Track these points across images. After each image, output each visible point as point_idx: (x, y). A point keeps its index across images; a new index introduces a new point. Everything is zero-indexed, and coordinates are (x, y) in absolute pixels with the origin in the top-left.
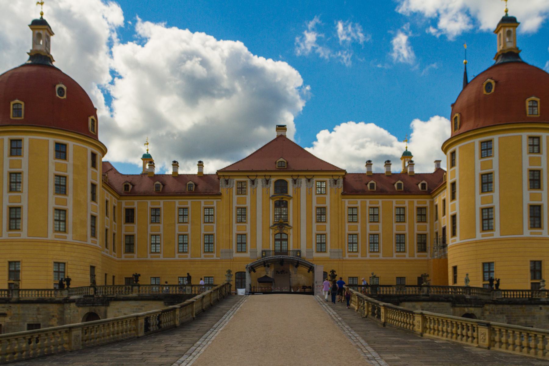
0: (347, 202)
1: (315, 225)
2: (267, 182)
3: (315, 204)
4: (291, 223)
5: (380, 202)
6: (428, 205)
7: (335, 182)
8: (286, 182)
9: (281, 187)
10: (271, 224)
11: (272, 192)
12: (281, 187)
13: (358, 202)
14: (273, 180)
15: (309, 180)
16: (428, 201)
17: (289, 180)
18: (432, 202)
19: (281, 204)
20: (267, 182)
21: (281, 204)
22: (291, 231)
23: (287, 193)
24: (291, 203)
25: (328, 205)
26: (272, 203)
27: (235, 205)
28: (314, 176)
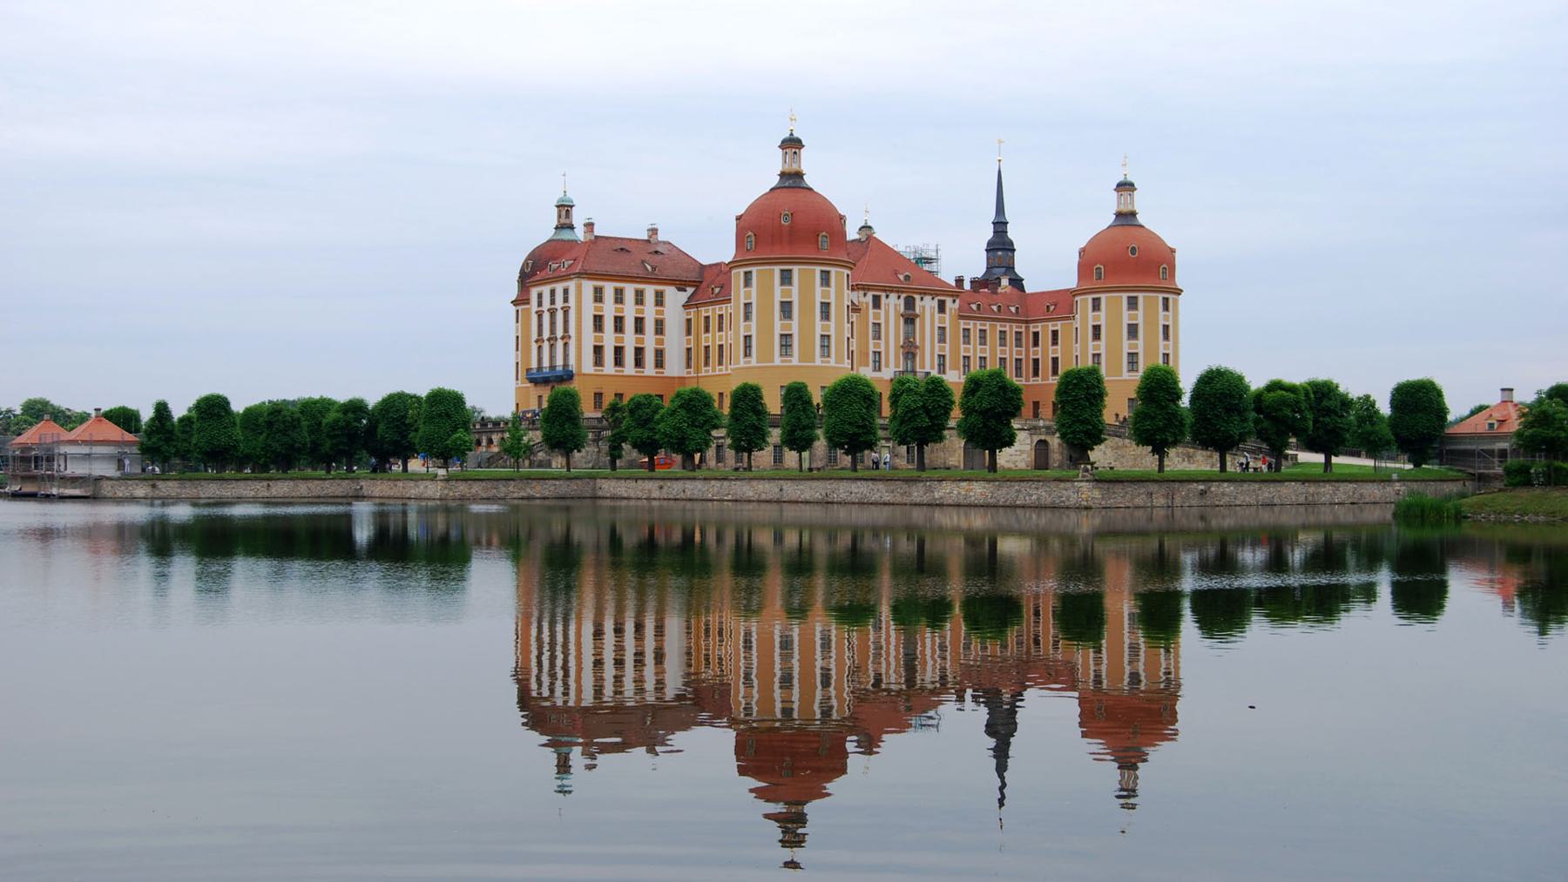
0: (962, 324)
1: (937, 345)
2: (899, 297)
3: (937, 324)
4: (918, 344)
5: (987, 326)
6: (1023, 330)
7: (954, 301)
8: (914, 299)
9: (910, 303)
10: (901, 343)
11: (902, 309)
12: (910, 303)
13: (971, 325)
14: (903, 296)
15: (933, 299)
16: (1024, 325)
17: (917, 297)
18: (1027, 328)
19: (910, 320)
20: (899, 297)
21: (910, 320)
22: (918, 351)
23: (914, 309)
24: (918, 321)
25: (947, 325)
26: (902, 320)
27: (871, 320)
28: (938, 295)
